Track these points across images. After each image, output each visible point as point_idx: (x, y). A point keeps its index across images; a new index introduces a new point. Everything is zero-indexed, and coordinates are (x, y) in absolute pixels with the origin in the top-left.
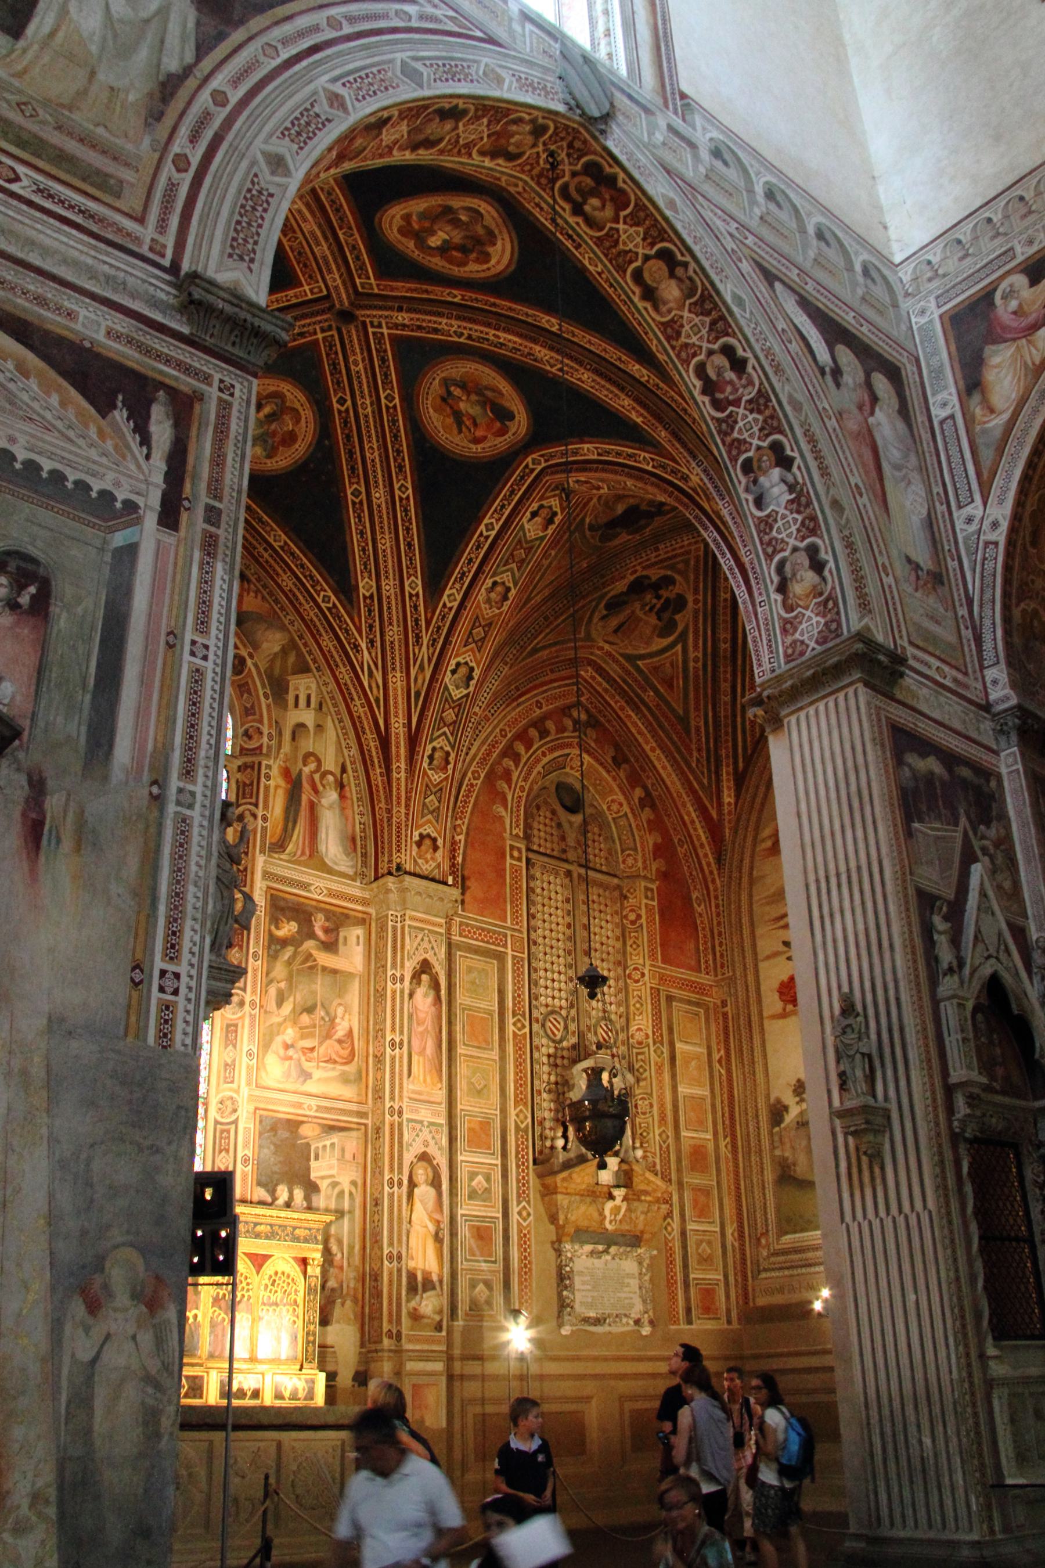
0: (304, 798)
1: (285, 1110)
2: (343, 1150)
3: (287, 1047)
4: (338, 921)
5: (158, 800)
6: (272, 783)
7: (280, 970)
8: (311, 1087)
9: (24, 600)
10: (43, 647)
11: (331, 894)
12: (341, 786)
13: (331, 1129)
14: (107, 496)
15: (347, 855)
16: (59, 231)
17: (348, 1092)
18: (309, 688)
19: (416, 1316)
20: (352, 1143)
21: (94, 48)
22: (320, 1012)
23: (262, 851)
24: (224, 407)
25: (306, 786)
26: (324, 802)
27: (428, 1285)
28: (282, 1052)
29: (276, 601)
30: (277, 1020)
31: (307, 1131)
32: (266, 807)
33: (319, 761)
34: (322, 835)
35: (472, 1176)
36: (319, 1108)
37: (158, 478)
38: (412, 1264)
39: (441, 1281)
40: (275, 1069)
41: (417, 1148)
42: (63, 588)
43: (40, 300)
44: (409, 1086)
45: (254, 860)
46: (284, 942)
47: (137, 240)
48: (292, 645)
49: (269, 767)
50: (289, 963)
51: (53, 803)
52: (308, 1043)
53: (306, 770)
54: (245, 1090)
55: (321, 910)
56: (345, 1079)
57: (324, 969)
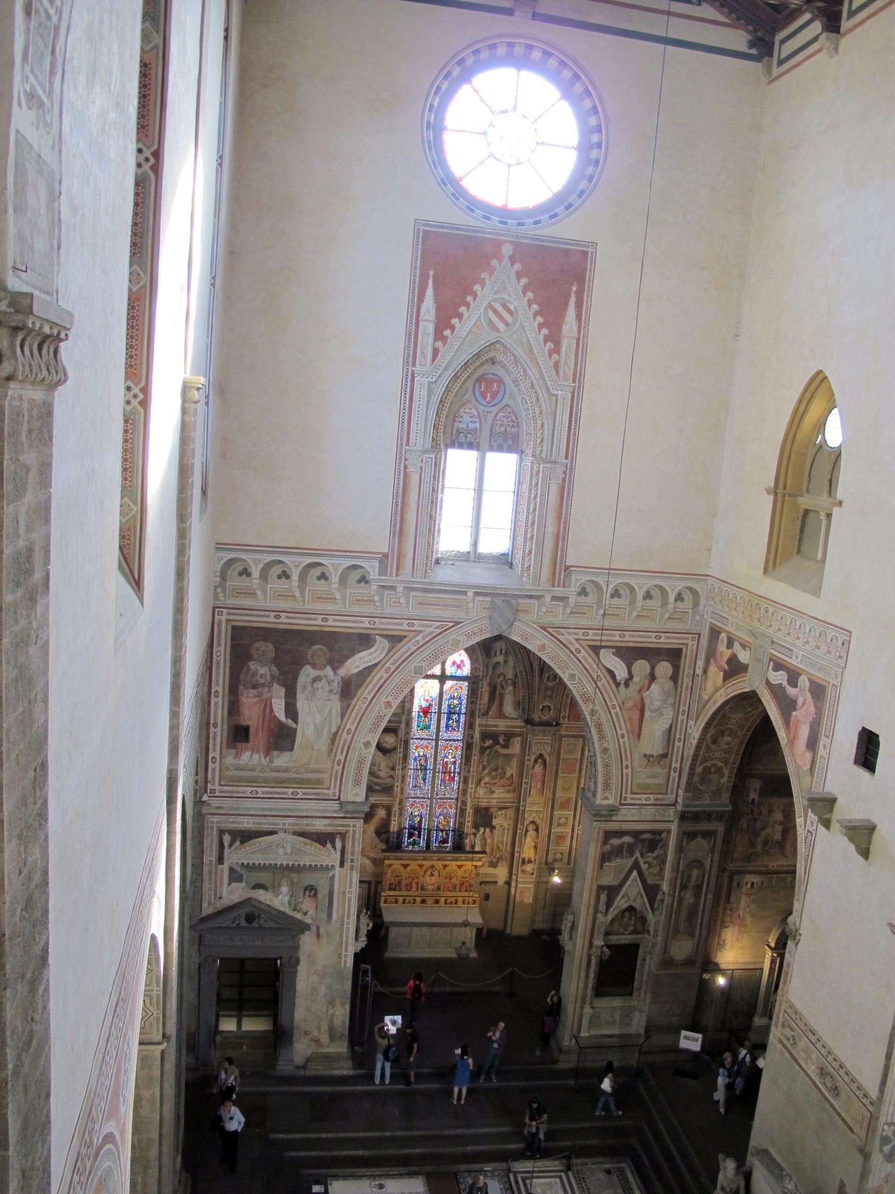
0: (498, 692)
1: (484, 804)
2: (506, 815)
3: (486, 783)
4: (509, 736)
5: (342, 925)
6: (483, 690)
7: (485, 758)
8: (495, 796)
9: (312, 894)
10: (317, 901)
11: (507, 727)
12: (514, 684)
13: (501, 808)
14: (327, 866)
15: (515, 710)
16: (309, 803)
17: (510, 796)
19: (524, 871)
20: (510, 813)
21: (312, 740)
22: (500, 770)
23: (479, 717)
24: (354, 831)
25: (498, 687)
26: (506, 692)
27: (530, 861)
28: (484, 786)
31: (492, 810)
32: (481, 700)
33: (505, 676)
34: (505, 705)
35: (560, 819)
36: (497, 802)
37: (339, 857)
38: (524, 856)
39: (535, 860)
40: (481, 791)
41: (531, 819)
42: (319, 889)
43: (308, 825)
44: (529, 799)
45: (475, 720)
47: (328, 795)
49: (483, 684)
50: (488, 755)
51: (321, 930)
52: (494, 782)
54: (469, 800)
55: (503, 734)
56: (508, 792)
57: (503, 755)
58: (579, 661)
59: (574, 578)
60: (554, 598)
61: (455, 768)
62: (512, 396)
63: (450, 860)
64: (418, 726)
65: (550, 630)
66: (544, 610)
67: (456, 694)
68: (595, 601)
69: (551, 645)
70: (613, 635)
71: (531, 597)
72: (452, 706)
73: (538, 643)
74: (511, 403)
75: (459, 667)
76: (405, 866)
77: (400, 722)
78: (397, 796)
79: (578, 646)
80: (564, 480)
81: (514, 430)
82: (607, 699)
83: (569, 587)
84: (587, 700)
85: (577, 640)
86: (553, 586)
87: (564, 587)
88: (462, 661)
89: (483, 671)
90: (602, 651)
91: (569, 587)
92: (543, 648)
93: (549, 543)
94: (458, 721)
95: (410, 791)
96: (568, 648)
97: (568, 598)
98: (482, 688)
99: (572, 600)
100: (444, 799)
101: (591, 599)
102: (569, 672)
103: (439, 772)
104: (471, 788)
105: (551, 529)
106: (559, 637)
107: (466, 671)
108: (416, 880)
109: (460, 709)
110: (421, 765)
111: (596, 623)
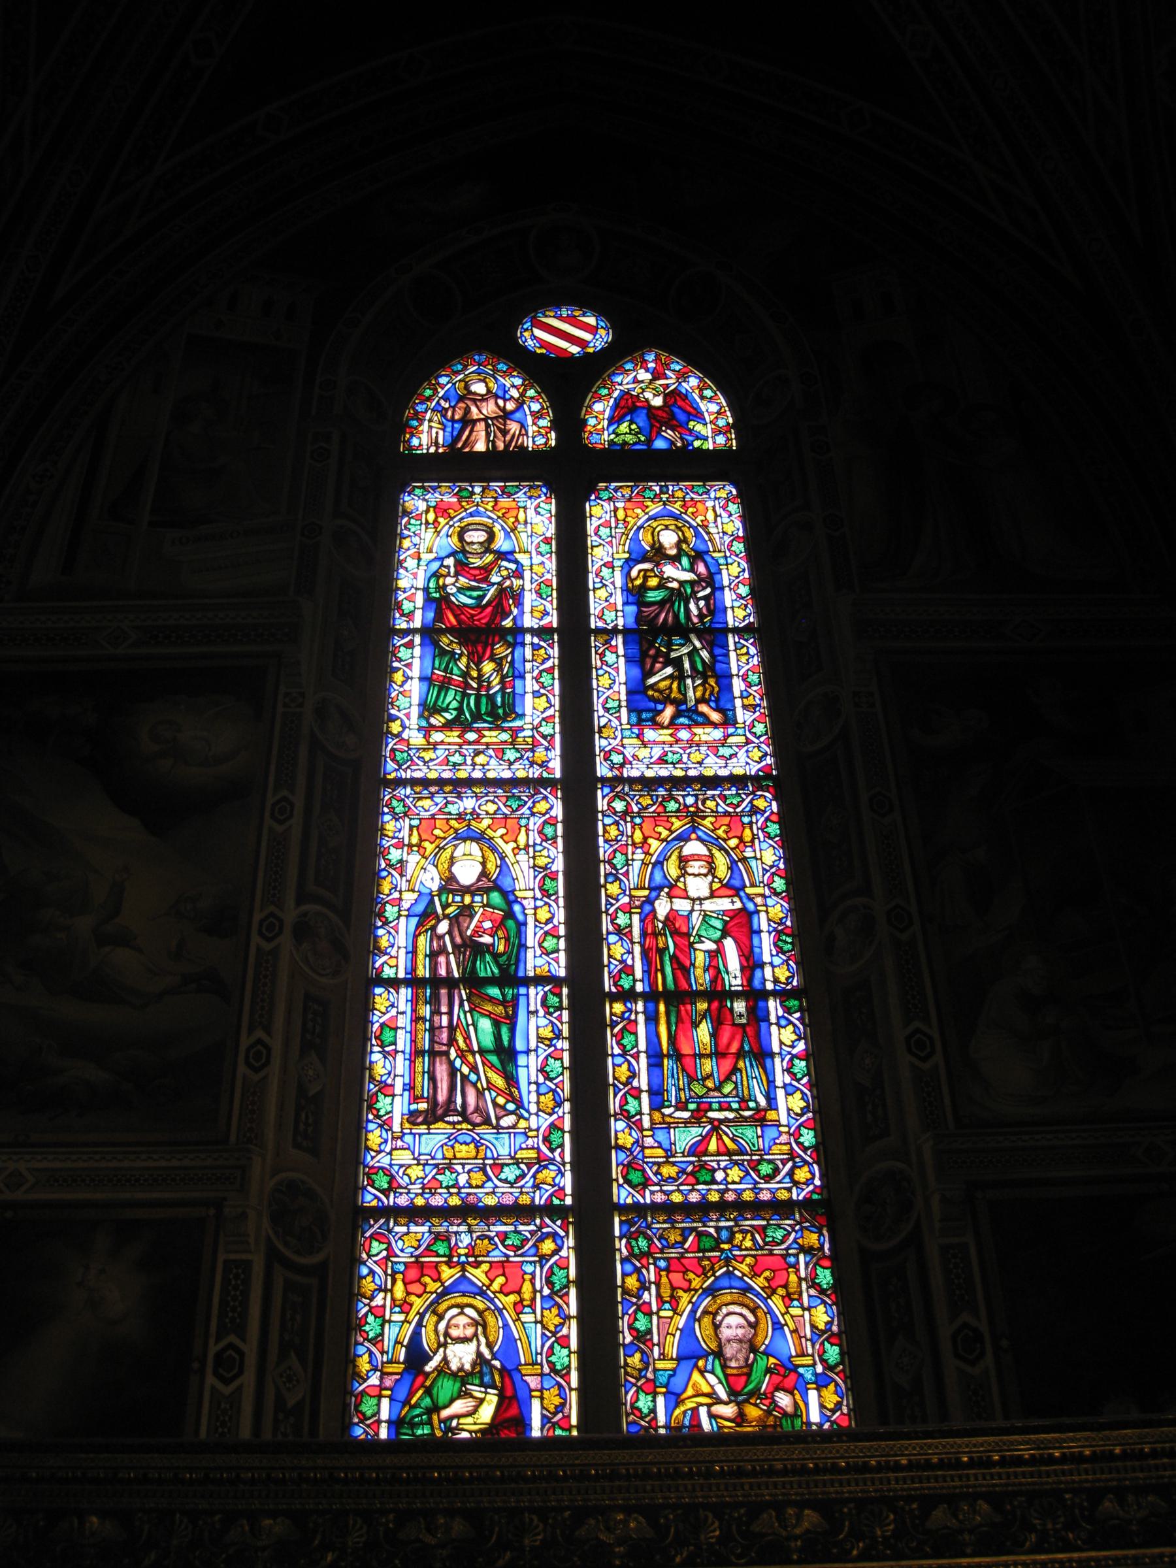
61: (751, 963)
64: (428, 709)
67: (668, 539)
72: (654, 596)
100: (704, 1208)
103: (628, 996)
109: (715, 608)
110: (471, 949)
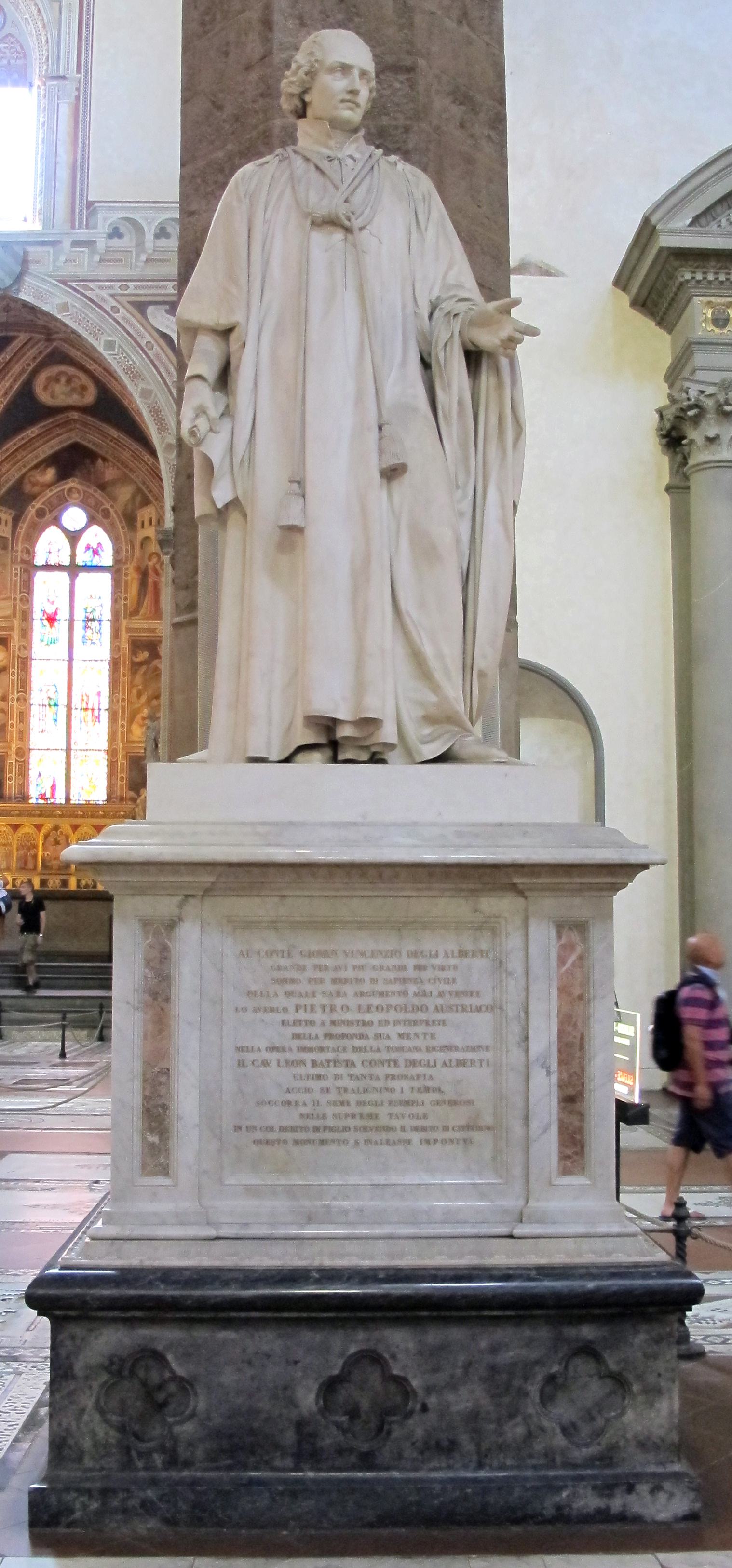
0: (150, 580)
3: (144, 719)
6: (129, 577)
18: (150, 513)
23: (125, 618)
25: (150, 571)
28: (141, 721)
29: (127, 467)
30: (137, 706)
46: (141, 664)
48: (139, 490)
49: (127, 569)
50: (145, 673)
53: (151, 564)
58: (118, 323)
59: (100, 216)
60: (76, 244)
62: (15, 24)
63: (82, 817)
65: (73, 284)
66: (62, 258)
68: (134, 244)
69: (76, 303)
70: (164, 287)
71: (43, 243)
72: (89, 610)
73: (58, 301)
74: (14, 31)
75: (95, 552)
76: (16, 827)
77: (11, 629)
78: (12, 740)
79: (114, 304)
80: (77, 98)
81: (19, 62)
82: (164, 374)
83: (95, 227)
84: (135, 376)
85: (112, 296)
86: (73, 227)
87: (87, 227)
88: (99, 545)
89: (127, 551)
90: (150, 310)
91: (95, 227)
92: (65, 307)
93: (63, 174)
94: (99, 632)
95: (36, 739)
96: (100, 307)
97: (94, 242)
98: (126, 575)
99: (101, 244)
101: (128, 241)
102: (105, 338)
104: (123, 726)
105: (64, 157)
106: (88, 293)
107: (107, 558)
108: (32, 852)
111: (136, 272)
